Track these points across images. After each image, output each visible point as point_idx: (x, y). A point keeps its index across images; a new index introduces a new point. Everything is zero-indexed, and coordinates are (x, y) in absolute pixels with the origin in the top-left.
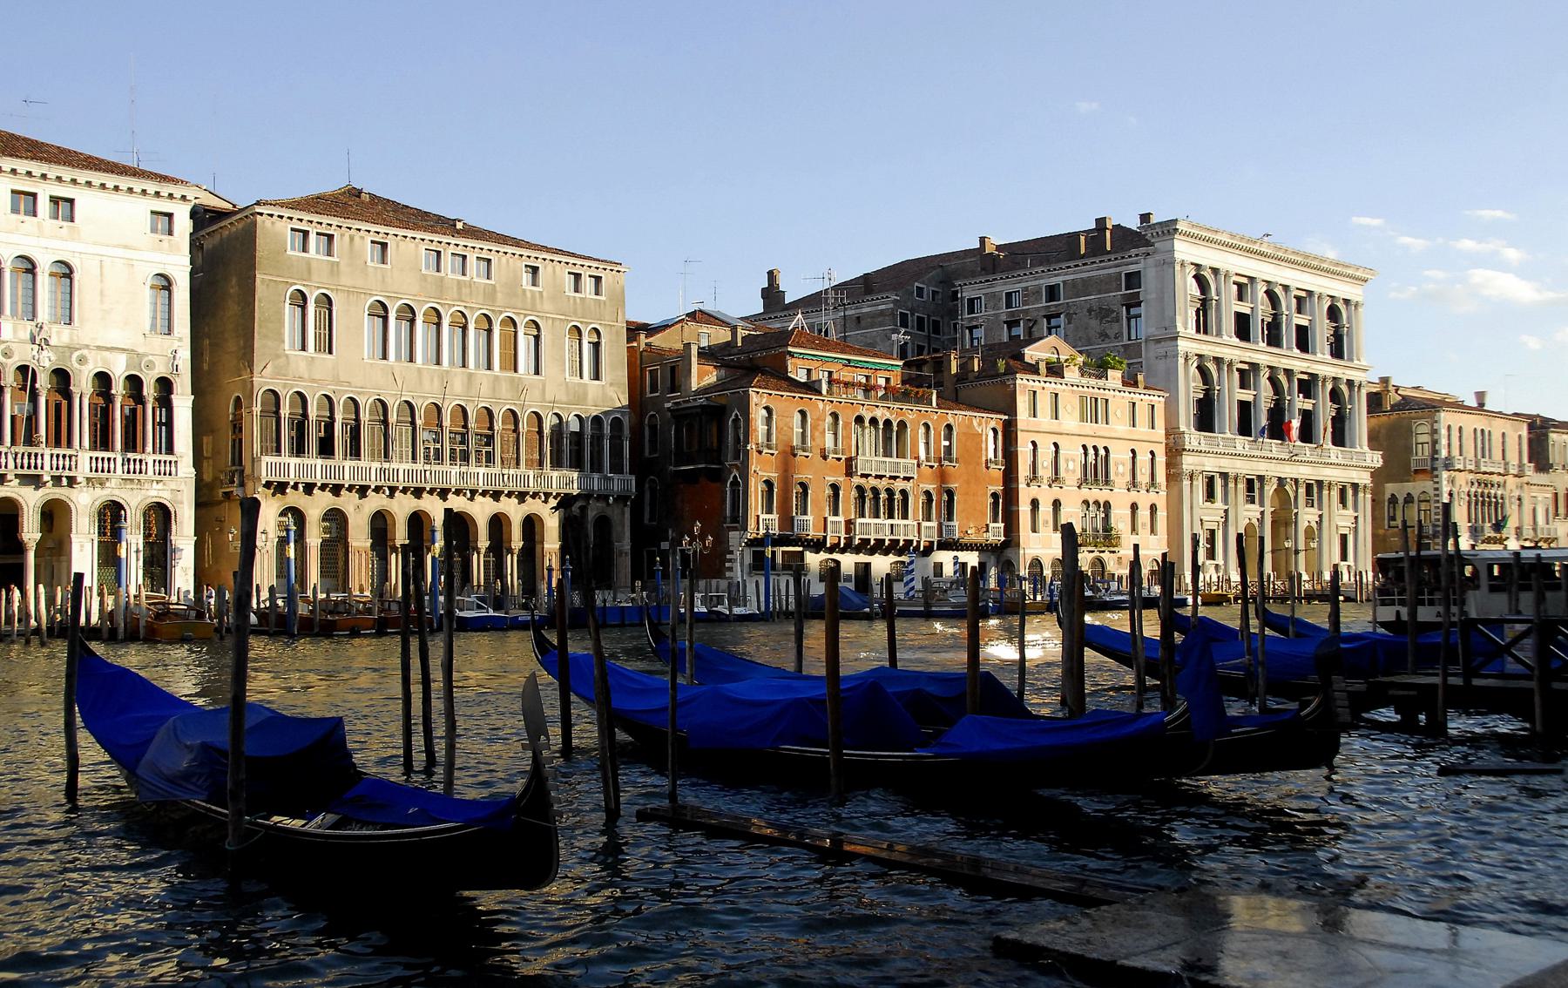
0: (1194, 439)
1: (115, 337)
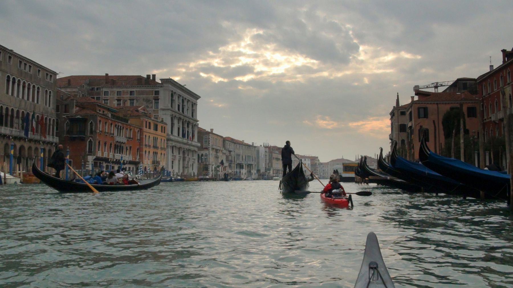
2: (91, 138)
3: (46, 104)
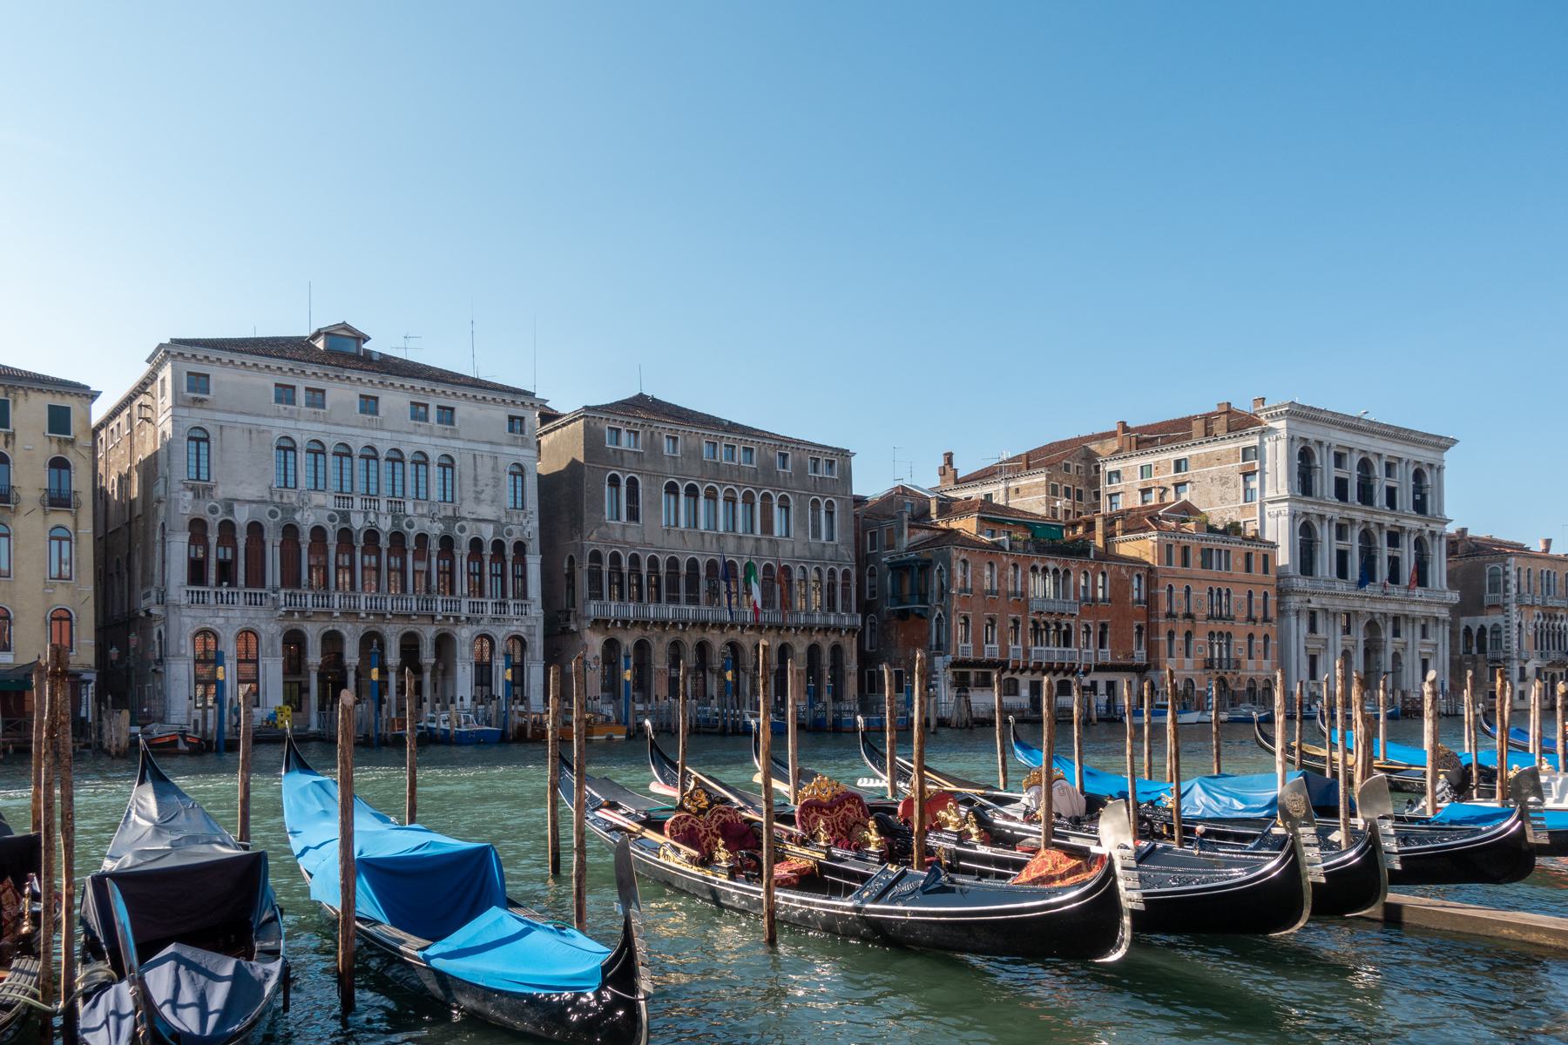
0: (1301, 583)
1: (487, 511)
2: (939, 610)
3: (816, 534)
